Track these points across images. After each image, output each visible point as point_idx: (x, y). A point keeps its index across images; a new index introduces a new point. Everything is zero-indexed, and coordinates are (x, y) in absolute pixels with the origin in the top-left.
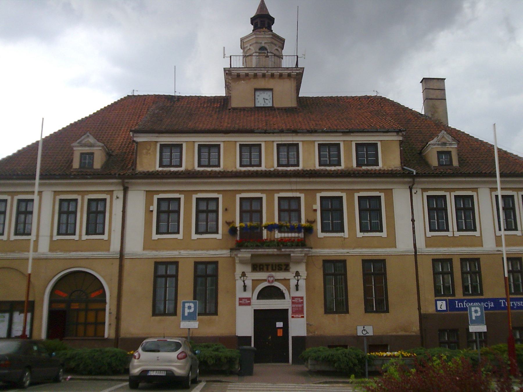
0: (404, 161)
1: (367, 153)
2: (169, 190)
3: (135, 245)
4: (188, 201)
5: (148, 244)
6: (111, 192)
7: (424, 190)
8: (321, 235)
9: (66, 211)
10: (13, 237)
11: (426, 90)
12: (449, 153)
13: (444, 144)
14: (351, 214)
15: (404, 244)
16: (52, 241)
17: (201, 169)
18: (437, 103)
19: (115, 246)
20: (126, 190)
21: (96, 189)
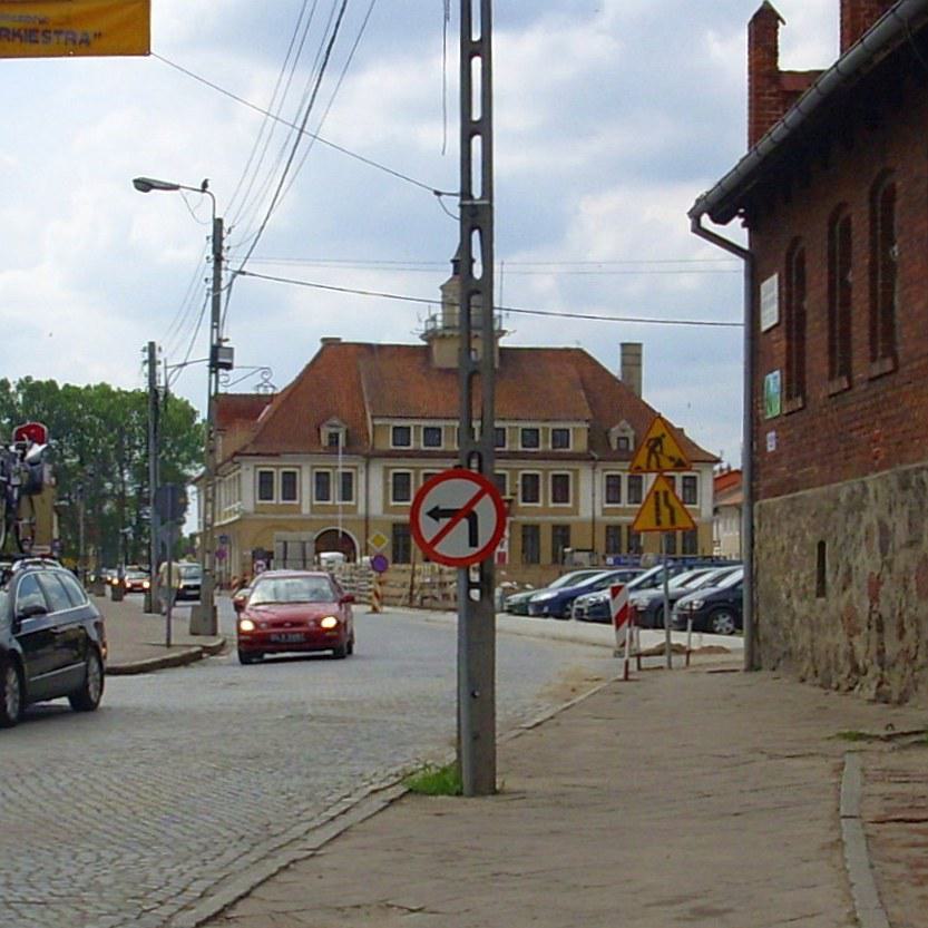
0: (591, 442)
1: (561, 437)
2: (402, 466)
3: (377, 509)
4: (417, 476)
5: (387, 508)
6: (355, 467)
7: (604, 470)
8: (522, 504)
9: (322, 482)
10: (281, 502)
11: (623, 354)
12: (627, 439)
13: (623, 431)
14: (546, 489)
15: (585, 513)
16: (312, 506)
17: (427, 448)
18: (634, 368)
19: (361, 510)
20: (367, 466)
21: (341, 464)
